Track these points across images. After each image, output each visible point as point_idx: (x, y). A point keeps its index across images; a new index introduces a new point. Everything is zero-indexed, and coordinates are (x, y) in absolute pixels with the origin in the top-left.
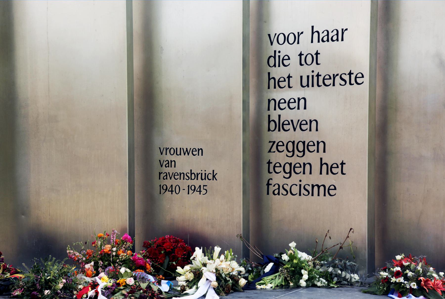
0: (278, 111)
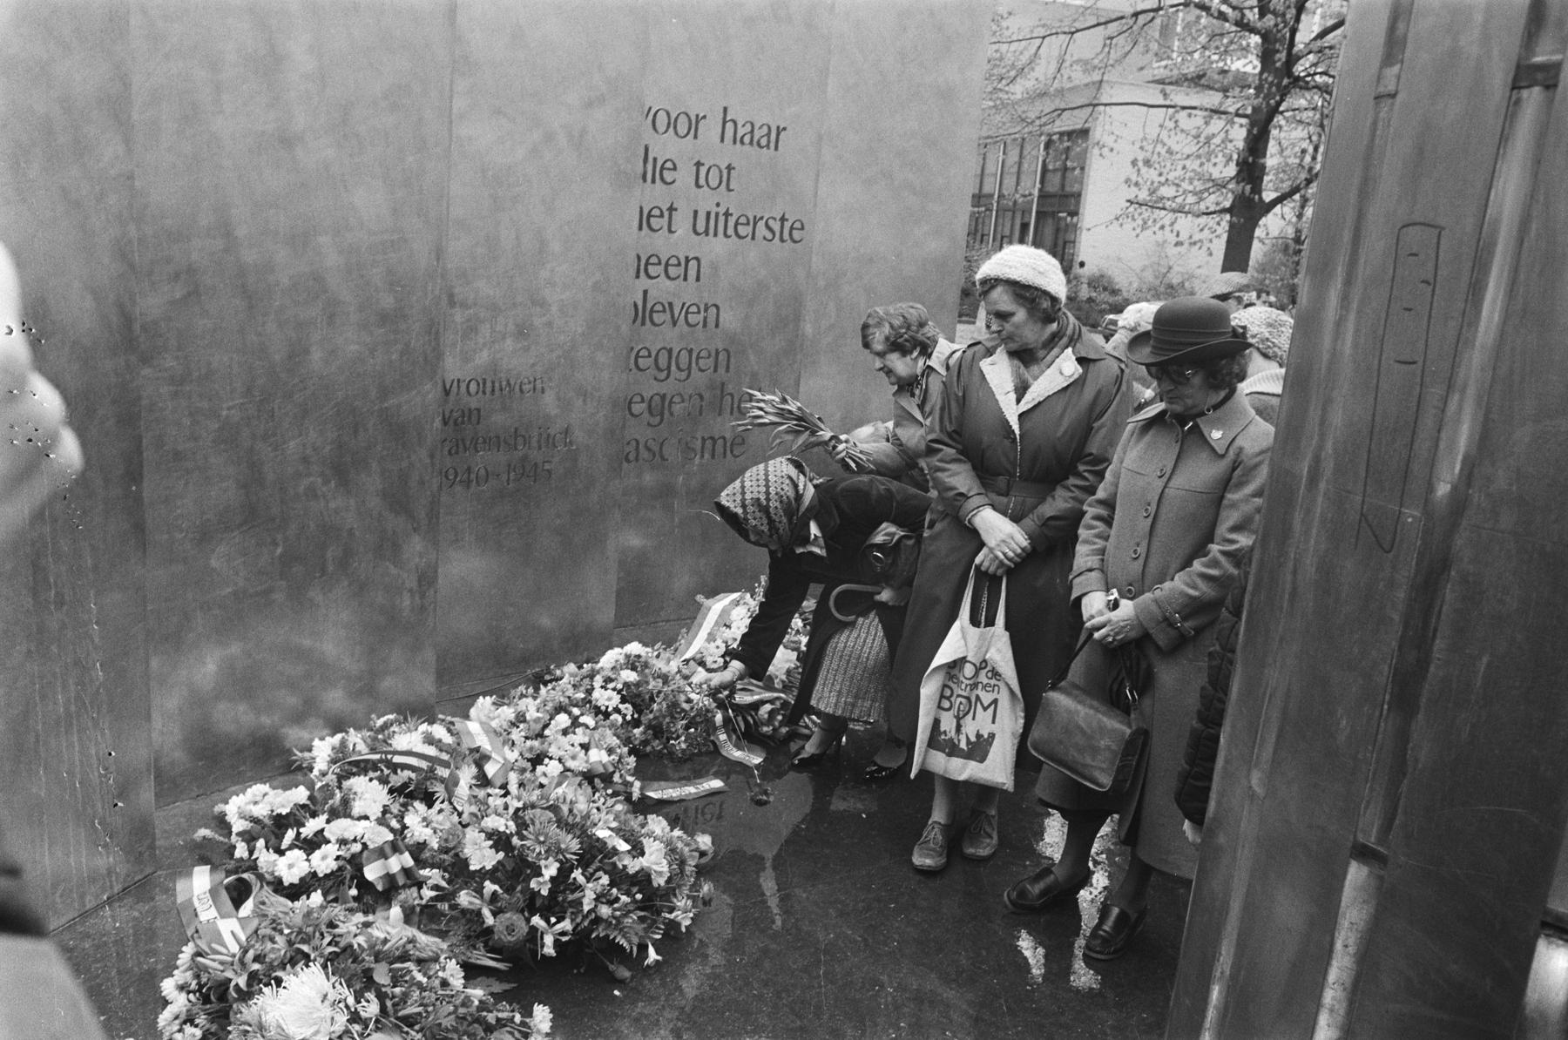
0: (644, 282)
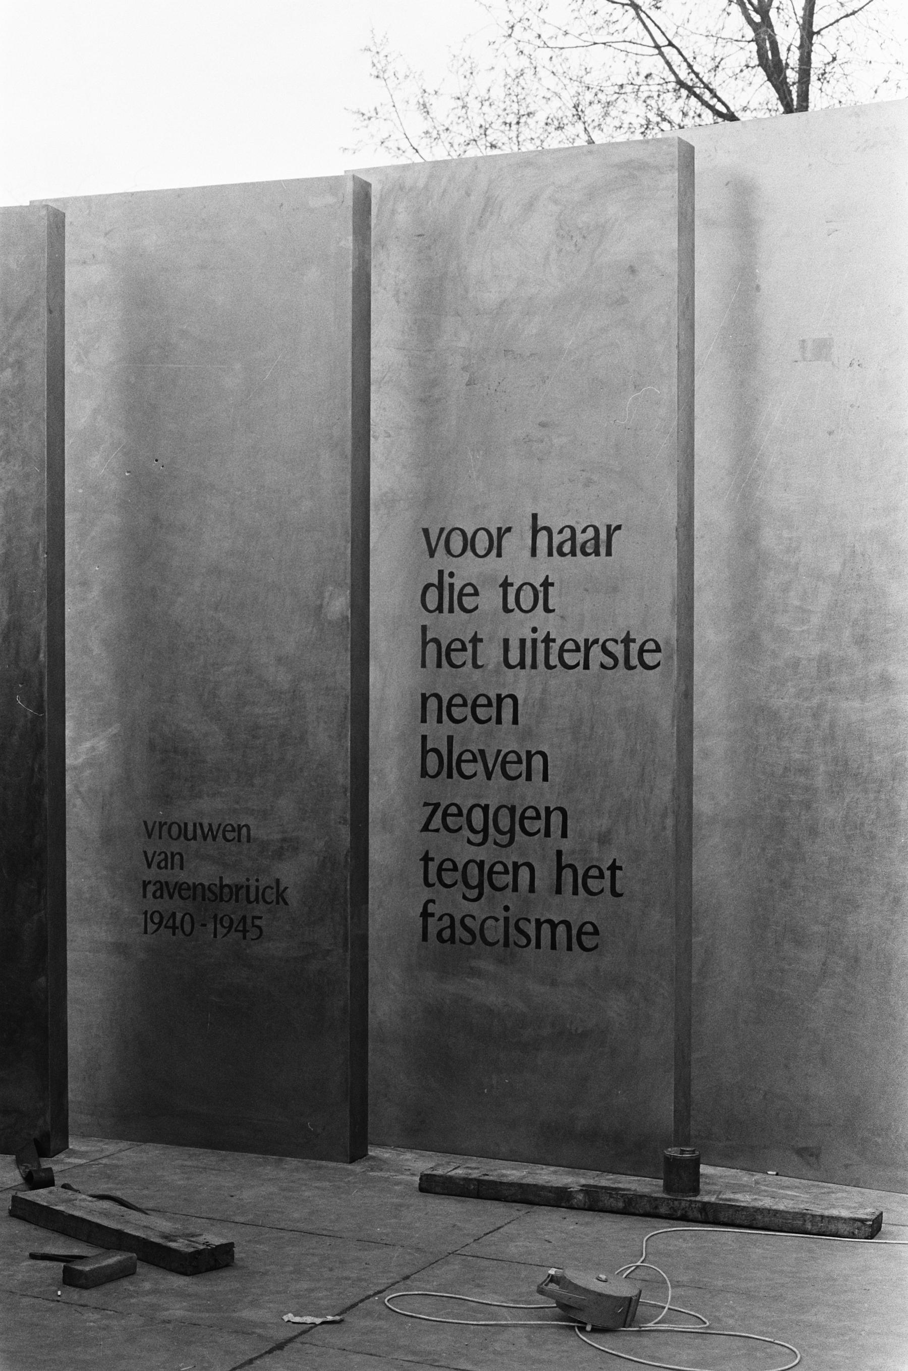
0: (448, 727)
